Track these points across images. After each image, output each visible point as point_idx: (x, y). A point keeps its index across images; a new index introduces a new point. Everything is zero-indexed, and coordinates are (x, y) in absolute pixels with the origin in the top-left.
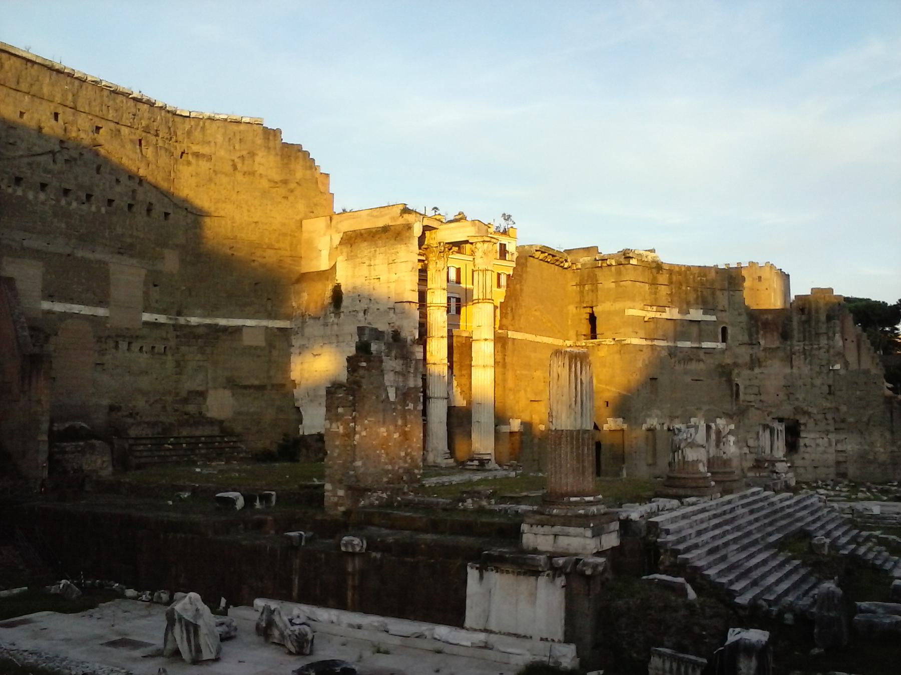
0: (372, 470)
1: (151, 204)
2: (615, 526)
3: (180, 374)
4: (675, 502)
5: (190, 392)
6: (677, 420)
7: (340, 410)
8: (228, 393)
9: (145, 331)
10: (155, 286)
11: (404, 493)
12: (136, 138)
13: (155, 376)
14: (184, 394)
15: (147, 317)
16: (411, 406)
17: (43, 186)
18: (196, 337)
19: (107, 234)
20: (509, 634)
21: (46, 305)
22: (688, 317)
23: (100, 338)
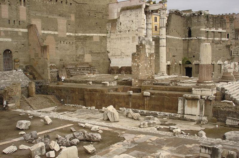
0: (143, 75)
1: (67, 1)
2: (216, 88)
3: (77, 50)
4: (226, 83)
5: (80, 55)
6: (214, 61)
7: (136, 59)
8: (90, 55)
9: (68, 38)
10: (69, 25)
11: (155, 81)
13: (71, 51)
14: (78, 56)
15: (68, 34)
16: (152, 58)
18: (81, 39)
19: (56, 11)
20: (190, 115)
21: (43, 32)
22: (218, 31)
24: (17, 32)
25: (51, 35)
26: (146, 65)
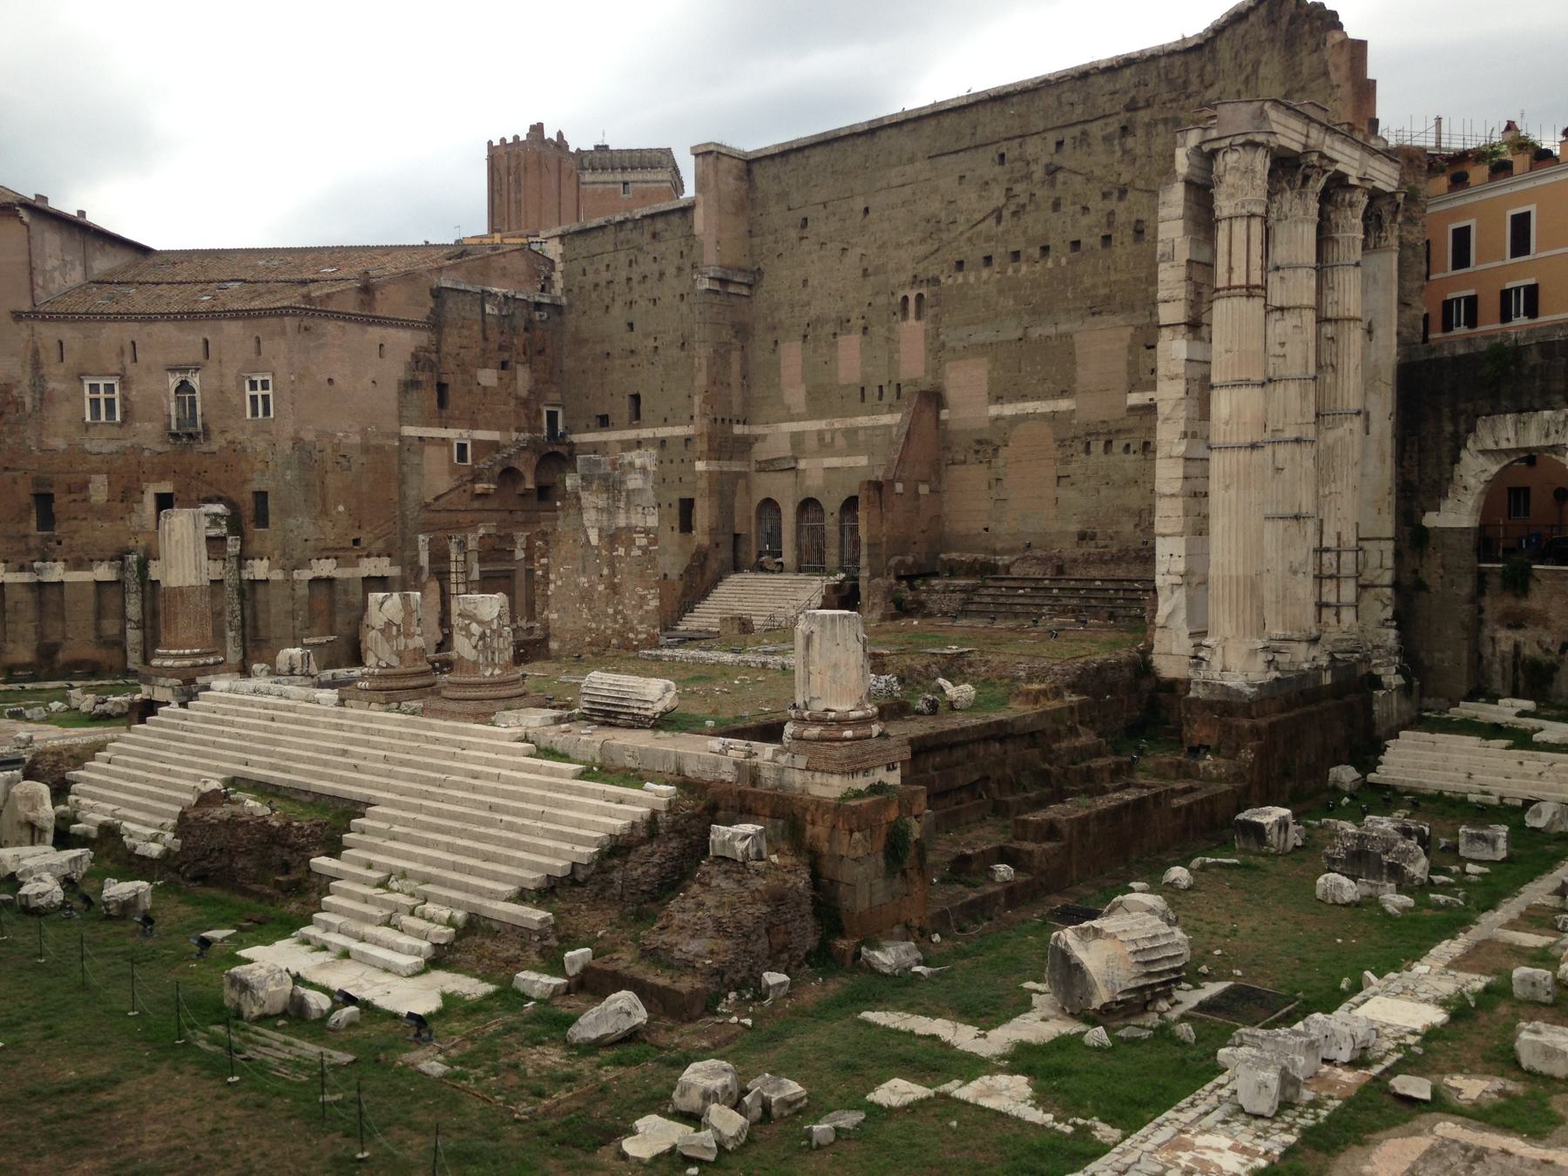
0: (570, 625)
1: (1139, 222)
9: (1132, 421)
12: (1114, 126)
16: (621, 551)
17: (988, 260)
21: (994, 410)
23: (1063, 441)
24: (888, 427)
26: (583, 579)
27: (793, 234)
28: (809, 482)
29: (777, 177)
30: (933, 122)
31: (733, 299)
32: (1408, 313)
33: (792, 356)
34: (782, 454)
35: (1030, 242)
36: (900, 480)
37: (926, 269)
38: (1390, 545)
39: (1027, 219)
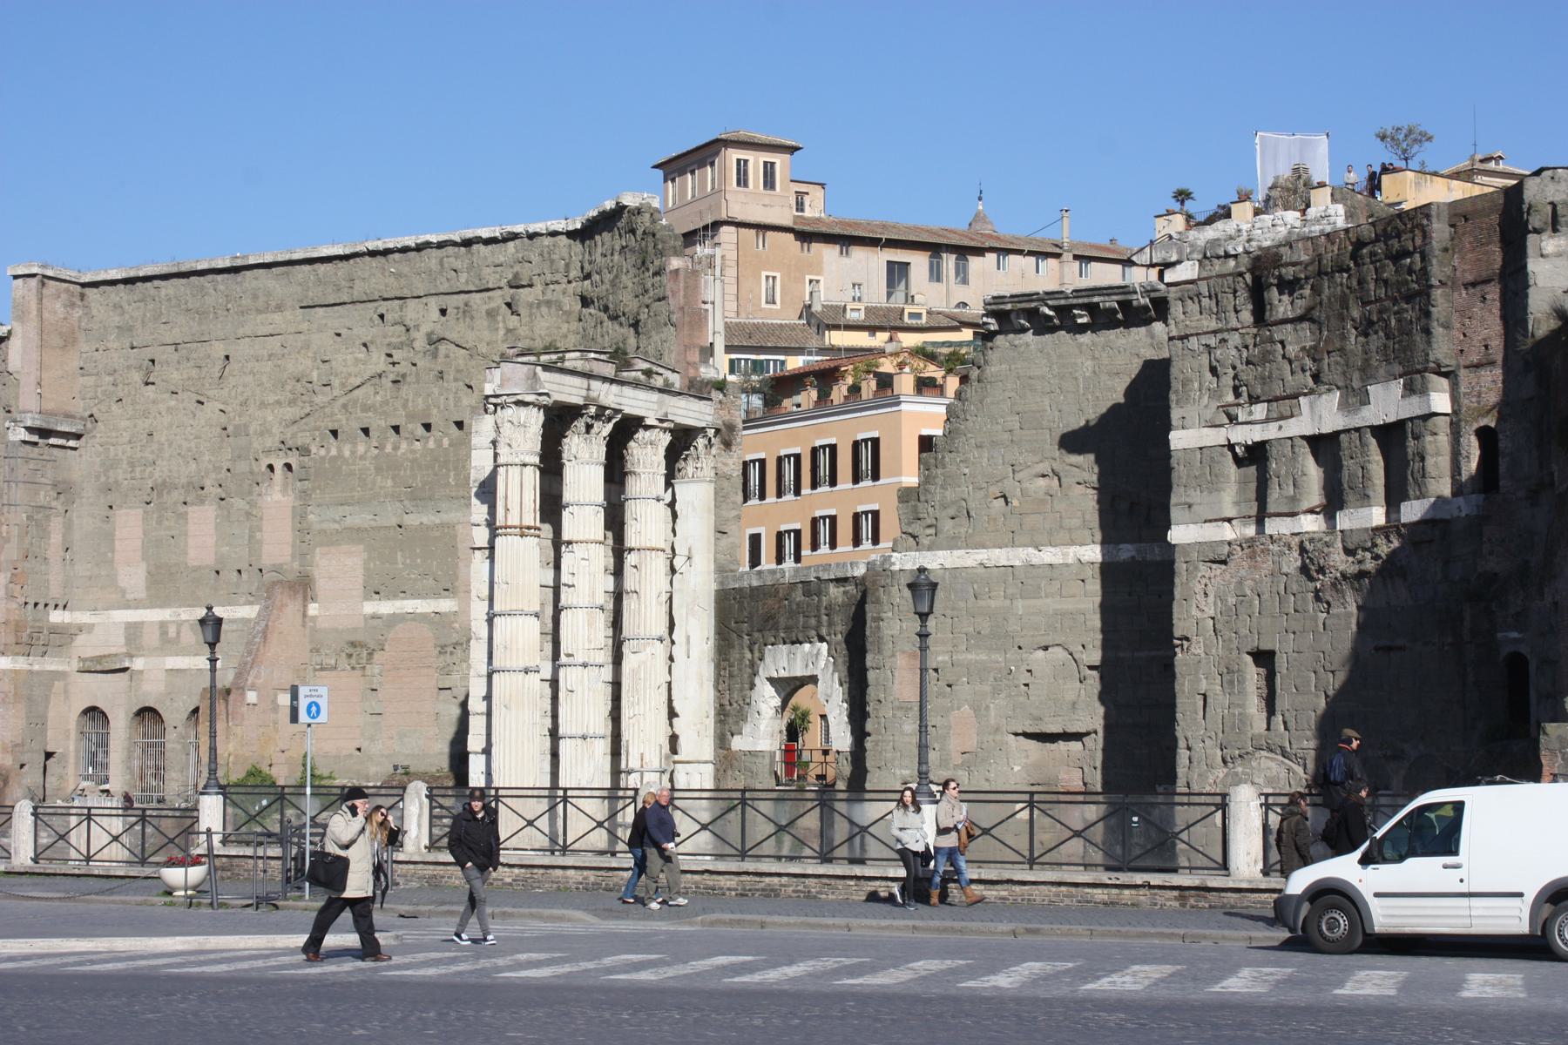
17: (366, 431)
21: (370, 607)
23: (443, 647)
24: (245, 621)
25: (413, 620)
27: (137, 377)
28: (147, 687)
29: (117, 307)
30: (306, 268)
31: (56, 451)
32: (725, 541)
33: (130, 524)
34: (113, 651)
35: (411, 417)
36: (253, 688)
37: (294, 436)
38: (710, 767)
39: (406, 391)
